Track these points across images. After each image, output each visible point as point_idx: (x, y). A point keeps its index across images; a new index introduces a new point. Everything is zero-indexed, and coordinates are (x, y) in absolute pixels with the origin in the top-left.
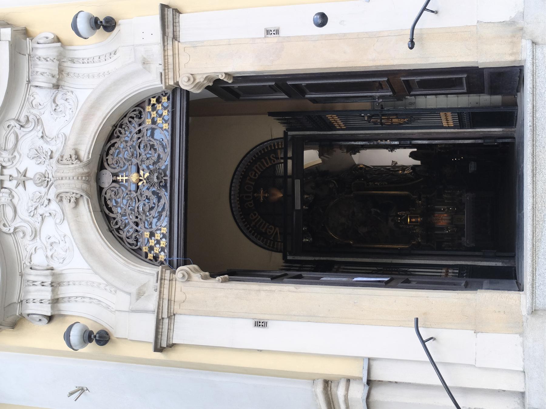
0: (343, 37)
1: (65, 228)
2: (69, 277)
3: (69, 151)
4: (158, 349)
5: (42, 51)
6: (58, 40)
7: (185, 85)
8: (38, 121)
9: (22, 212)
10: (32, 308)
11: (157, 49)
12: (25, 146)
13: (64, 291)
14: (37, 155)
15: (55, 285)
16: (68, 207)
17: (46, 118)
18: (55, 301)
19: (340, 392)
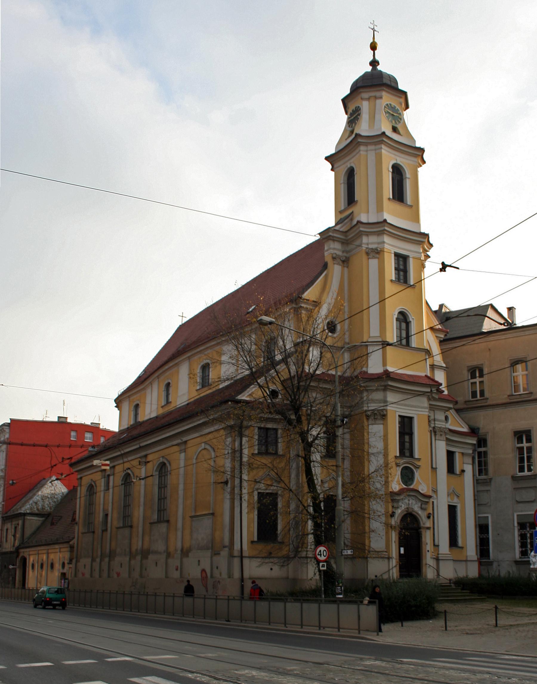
0: (426, 554)
8: (416, 504)
14: (412, 503)
16: (406, 510)
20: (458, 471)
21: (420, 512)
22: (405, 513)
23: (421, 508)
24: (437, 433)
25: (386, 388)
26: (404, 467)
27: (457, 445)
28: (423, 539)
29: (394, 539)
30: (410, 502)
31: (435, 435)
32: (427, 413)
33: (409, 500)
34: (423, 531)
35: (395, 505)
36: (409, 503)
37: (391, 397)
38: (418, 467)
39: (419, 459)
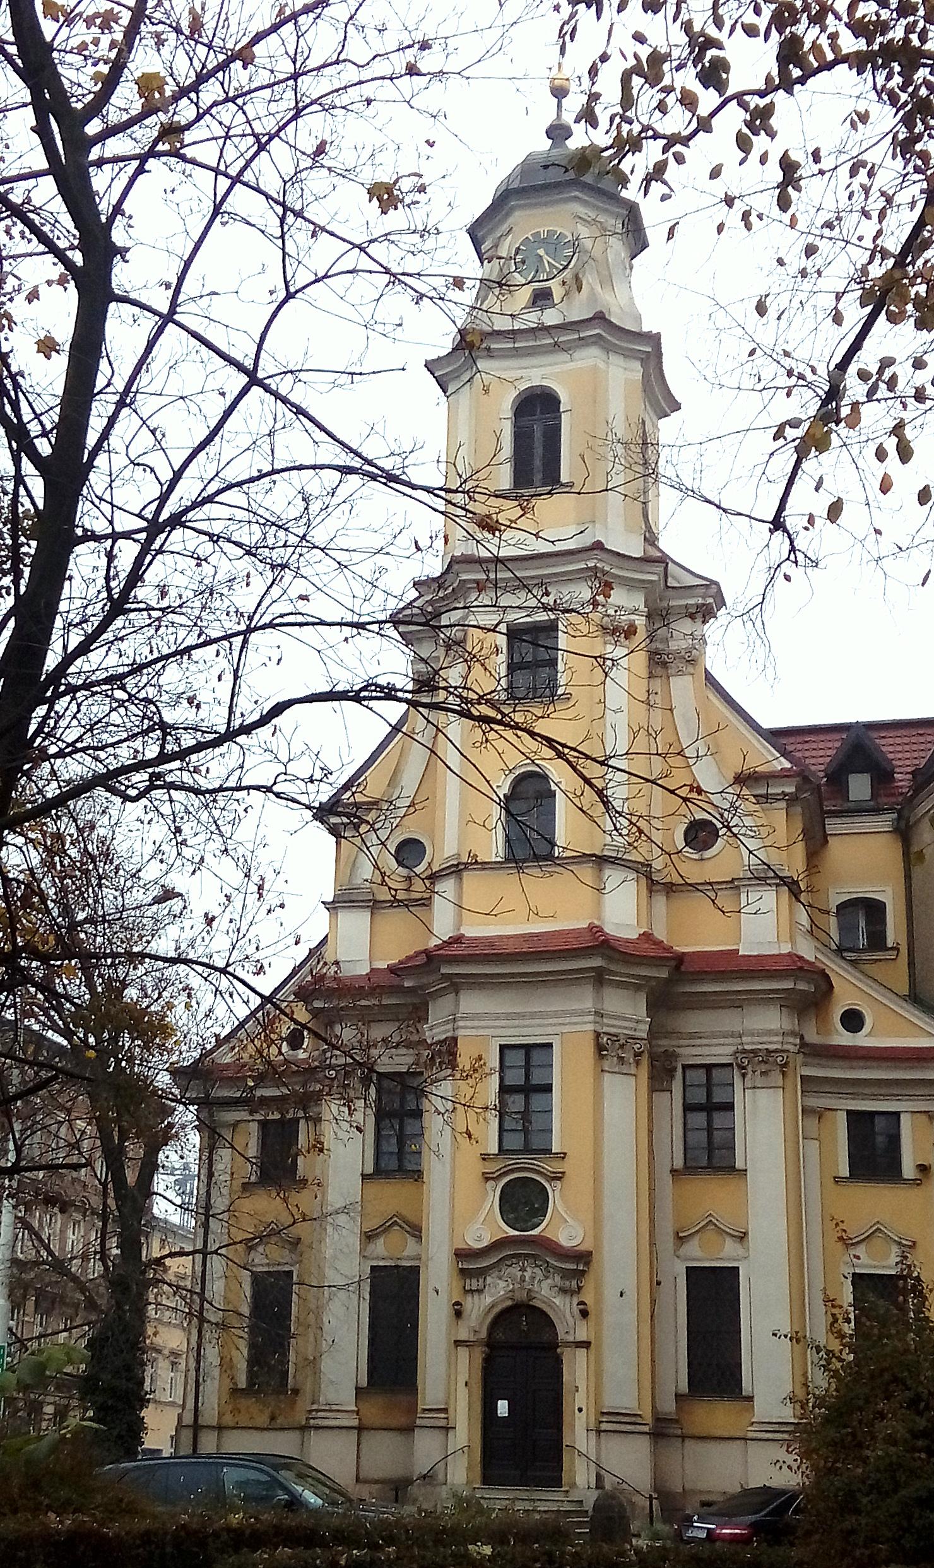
1: (502, 1293)
2: (482, 1297)
3: (534, 1295)
4: (455, 1342)
5: (574, 1283)
6: (580, 1288)
7: (559, 1350)
8: (547, 1278)
9: (510, 1269)
10: (468, 1281)
11: (571, 1338)
12: (537, 1270)
13: (476, 1297)
15: (477, 1290)
17: (549, 1281)
18: (471, 1291)
19: (443, 1415)
20: (908, 1170)
21: (557, 1301)
22: (509, 1303)
23: (563, 1291)
24: (750, 1068)
25: (455, 985)
26: (507, 1184)
27: (867, 1091)
28: (566, 1377)
29: (463, 1378)
30: (527, 1275)
31: (744, 1076)
32: (591, 1027)
33: (523, 1270)
34: (566, 1354)
35: (475, 1284)
36: (523, 1277)
37: (471, 1003)
38: (558, 1177)
39: (563, 1156)
